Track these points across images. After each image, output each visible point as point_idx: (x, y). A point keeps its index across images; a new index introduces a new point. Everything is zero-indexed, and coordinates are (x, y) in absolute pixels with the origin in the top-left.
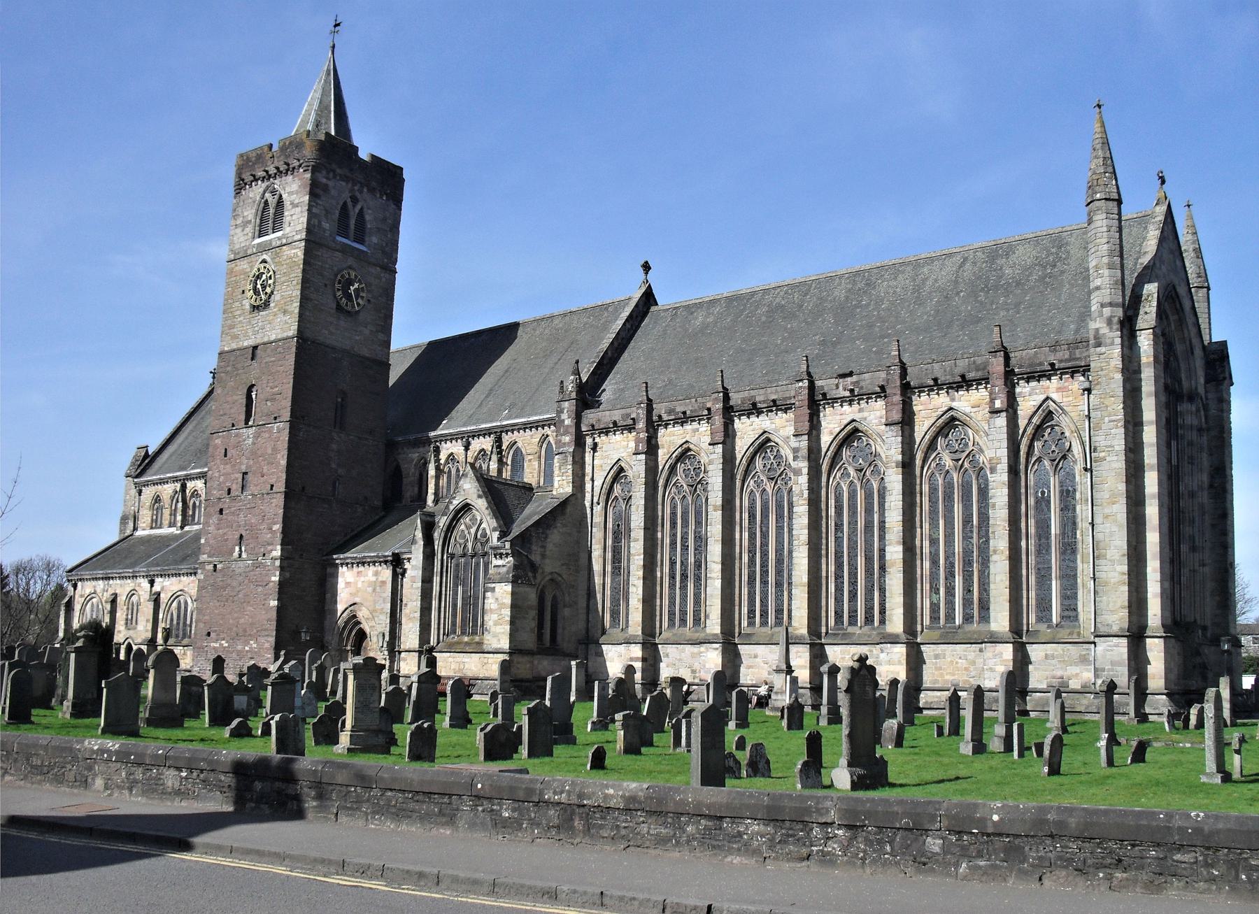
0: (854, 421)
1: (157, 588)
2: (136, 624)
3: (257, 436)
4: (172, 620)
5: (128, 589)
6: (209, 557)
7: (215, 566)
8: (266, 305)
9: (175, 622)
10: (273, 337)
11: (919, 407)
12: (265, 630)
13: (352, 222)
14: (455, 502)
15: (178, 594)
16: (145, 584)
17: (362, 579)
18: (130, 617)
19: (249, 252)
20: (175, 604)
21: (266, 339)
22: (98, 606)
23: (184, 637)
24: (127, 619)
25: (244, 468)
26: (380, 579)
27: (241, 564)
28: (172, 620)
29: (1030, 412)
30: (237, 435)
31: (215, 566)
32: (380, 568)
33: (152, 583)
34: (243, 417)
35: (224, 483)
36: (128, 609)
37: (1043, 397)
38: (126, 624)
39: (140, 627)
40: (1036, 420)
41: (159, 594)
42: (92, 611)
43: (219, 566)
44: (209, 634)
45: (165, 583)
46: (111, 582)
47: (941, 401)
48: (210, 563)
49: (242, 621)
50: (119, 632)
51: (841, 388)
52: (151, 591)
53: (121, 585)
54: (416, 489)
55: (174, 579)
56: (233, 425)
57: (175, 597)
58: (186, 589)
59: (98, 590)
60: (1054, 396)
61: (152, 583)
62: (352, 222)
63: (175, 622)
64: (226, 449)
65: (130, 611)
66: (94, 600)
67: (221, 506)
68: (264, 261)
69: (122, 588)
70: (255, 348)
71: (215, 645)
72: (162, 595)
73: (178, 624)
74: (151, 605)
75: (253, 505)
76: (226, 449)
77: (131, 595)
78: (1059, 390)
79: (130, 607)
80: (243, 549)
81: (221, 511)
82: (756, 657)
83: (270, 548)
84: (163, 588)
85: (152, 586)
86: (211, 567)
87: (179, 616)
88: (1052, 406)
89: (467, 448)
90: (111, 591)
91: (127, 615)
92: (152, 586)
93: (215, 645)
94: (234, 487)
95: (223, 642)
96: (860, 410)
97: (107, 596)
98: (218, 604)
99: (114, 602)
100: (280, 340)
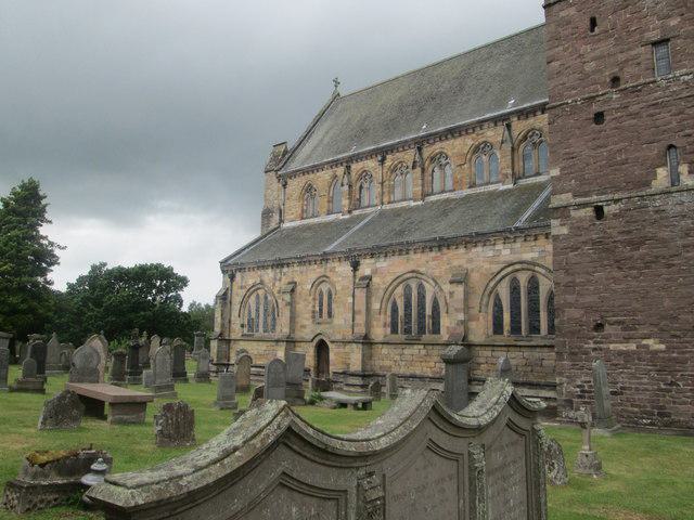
1: (366, 268)
6: (575, 196)
7: (599, 211)
9: (401, 312)
15: (405, 276)
16: (345, 268)
18: (317, 309)
20: (400, 290)
22: (266, 298)
23: (422, 330)
24: (314, 312)
25: (655, 35)
28: (395, 310)
31: (599, 211)
33: (355, 266)
35: (598, 71)
36: (314, 299)
38: (314, 317)
42: (258, 303)
44: (599, 327)
45: (378, 265)
46: (285, 269)
50: (303, 327)
52: (355, 276)
53: (301, 273)
57: (400, 280)
58: (422, 270)
61: (355, 266)
63: (401, 312)
65: (317, 302)
66: (261, 292)
67: (595, 108)
69: (306, 277)
72: (374, 280)
73: (408, 315)
74: (361, 294)
77: (323, 279)
79: (318, 297)
81: (599, 118)
84: (375, 271)
86: (589, 212)
87: (408, 305)
90: (285, 280)
91: (314, 306)
93: (622, 347)
95: (650, 342)
97: (283, 284)
98: (619, 274)
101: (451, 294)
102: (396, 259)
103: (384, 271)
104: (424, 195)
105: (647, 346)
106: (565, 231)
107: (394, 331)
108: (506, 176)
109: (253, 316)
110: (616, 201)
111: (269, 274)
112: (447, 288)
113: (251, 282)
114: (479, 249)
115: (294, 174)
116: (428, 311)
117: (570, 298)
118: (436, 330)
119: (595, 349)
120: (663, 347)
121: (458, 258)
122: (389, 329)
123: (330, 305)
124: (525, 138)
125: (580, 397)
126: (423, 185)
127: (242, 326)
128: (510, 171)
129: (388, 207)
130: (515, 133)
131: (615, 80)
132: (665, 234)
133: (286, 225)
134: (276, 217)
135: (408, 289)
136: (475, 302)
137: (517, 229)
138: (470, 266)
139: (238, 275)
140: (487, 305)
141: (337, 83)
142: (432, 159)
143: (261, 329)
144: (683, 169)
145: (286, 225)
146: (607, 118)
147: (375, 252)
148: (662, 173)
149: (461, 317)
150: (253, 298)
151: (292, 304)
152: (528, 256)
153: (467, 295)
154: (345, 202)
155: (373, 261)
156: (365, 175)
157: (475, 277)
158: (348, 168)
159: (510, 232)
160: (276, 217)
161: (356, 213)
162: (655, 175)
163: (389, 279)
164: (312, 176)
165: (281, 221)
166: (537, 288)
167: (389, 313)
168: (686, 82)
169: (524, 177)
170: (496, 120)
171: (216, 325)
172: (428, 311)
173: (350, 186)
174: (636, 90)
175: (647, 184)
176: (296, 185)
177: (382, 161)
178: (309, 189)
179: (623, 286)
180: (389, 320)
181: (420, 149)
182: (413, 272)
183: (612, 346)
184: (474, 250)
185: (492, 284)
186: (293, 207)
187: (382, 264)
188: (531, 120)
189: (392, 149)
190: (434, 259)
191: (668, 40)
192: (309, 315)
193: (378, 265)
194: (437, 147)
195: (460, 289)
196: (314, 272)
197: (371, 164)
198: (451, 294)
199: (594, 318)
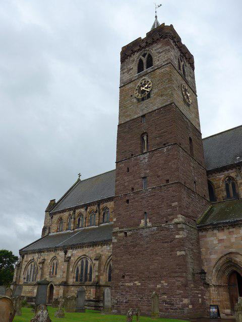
1: (69, 254)
2: (56, 274)
3: (150, 158)
4: (78, 271)
5: (52, 256)
7: (126, 233)
8: (149, 96)
9: (80, 272)
10: (156, 108)
12: (175, 272)
13: (182, 68)
16: (62, 253)
17: (235, 236)
18: (52, 271)
20: (80, 263)
21: (150, 111)
22: (34, 266)
23: (86, 280)
25: (143, 175)
28: (78, 271)
30: (136, 160)
31: (126, 233)
33: (66, 253)
34: (139, 149)
35: (128, 186)
38: (50, 274)
39: (58, 276)
41: (70, 258)
42: (31, 268)
43: (129, 233)
44: (123, 277)
45: (73, 252)
46: (42, 254)
48: (121, 232)
49: (152, 267)
52: (65, 257)
53: (48, 255)
54: (225, 194)
55: (79, 250)
56: (132, 155)
57: (80, 258)
59: (35, 258)
61: (66, 253)
62: (182, 68)
63: (80, 272)
64: (128, 168)
65: (52, 268)
66: (33, 263)
67: (127, 198)
69: (48, 256)
70: (143, 116)
71: (129, 284)
72: (72, 258)
73: (82, 273)
74: (66, 264)
75: (154, 194)
76: (128, 168)
77: (55, 258)
79: (52, 266)
80: (148, 220)
81: (128, 201)
83: (170, 217)
84: (72, 255)
85: (66, 254)
86: (122, 234)
87: (82, 270)
90: (42, 258)
91: (50, 270)
92: (66, 254)
93: (129, 284)
94: (137, 186)
95: (137, 282)
98: (130, 257)
99: (43, 263)
100: (161, 108)
101: (95, 264)
102: (79, 250)
103: (75, 254)
104: (99, 224)
105: (136, 284)
106: (116, 241)
107: (77, 280)
109: (29, 274)
110: (130, 231)
111: (36, 256)
112: (94, 262)
113: (29, 259)
114: (105, 246)
115: (55, 213)
116: (88, 272)
117: (116, 266)
118: (90, 280)
119: (122, 285)
120: (140, 284)
121: (98, 250)
122: (75, 279)
123: (56, 269)
125: (117, 304)
126: (99, 220)
127: (24, 279)
129: (87, 228)
131: (133, 189)
132: (142, 243)
133: (51, 234)
134: (47, 231)
135: (82, 262)
136: (102, 268)
138: (102, 253)
139: (25, 256)
140: (107, 269)
141: (80, 175)
142: (103, 209)
143: (31, 280)
144: (148, 220)
145: (50, 234)
146: (130, 202)
147: (73, 247)
148: (143, 221)
149: (97, 274)
150: (30, 266)
151: (42, 269)
153: (100, 265)
154: (72, 225)
155: (72, 250)
156: (81, 214)
157: (103, 257)
158: (74, 211)
160: (47, 231)
161: (76, 230)
162: (140, 222)
163: (76, 258)
164: (62, 214)
165: (49, 233)
167: (75, 273)
168: (149, 191)
171: (14, 278)
172: (88, 272)
173: (74, 219)
174: (137, 193)
175: (139, 225)
176: (56, 217)
177: (86, 209)
178: (61, 219)
179: (130, 261)
180: (75, 275)
181: (99, 205)
182: (84, 255)
183: (126, 284)
184: (104, 247)
185: (108, 261)
186: (54, 227)
187: (75, 252)
189: (89, 205)
190: (91, 250)
191: (146, 177)
192: (48, 274)
193: (73, 252)
194: (105, 205)
195: (97, 262)
196: (52, 255)
197: (83, 210)
198: (95, 264)
199: (122, 274)
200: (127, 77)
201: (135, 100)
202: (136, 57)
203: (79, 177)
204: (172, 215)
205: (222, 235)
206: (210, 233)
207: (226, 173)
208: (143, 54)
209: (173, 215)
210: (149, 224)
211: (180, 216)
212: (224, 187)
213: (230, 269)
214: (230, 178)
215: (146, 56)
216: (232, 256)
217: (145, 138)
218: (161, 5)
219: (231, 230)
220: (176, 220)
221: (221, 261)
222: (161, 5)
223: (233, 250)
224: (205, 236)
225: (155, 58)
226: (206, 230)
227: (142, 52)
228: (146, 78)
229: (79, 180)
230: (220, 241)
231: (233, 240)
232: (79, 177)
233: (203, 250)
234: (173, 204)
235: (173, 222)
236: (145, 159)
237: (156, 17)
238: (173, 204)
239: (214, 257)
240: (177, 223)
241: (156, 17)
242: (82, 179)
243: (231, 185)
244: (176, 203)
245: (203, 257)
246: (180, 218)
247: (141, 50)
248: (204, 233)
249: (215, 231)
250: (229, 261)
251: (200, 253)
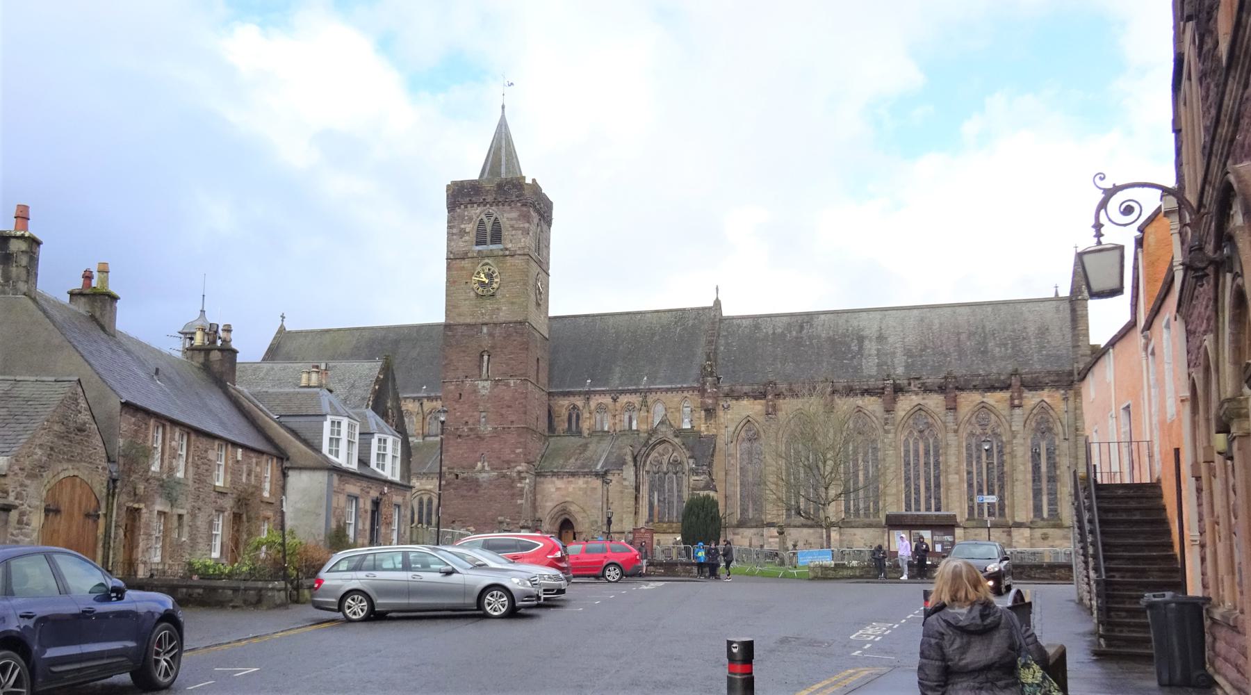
0: (920, 404)
11: (962, 400)
14: (653, 439)
17: (573, 486)
19: (469, 255)
26: (590, 486)
27: (484, 475)
29: (1032, 406)
31: (457, 476)
32: (590, 479)
37: (1039, 400)
40: (1035, 411)
47: (976, 397)
51: (912, 385)
60: (1046, 399)
64: (460, 394)
68: (487, 264)
78: (1049, 396)
82: (855, 535)
83: (513, 465)
88: (1045, 405)
89: (615, 400)
96: (924, 399)
108: (418, 434)
124: (431, 412)
128: (421, 432)
130: (425, 409)
137: (424, 473)
141: (283, 317)
144: (486, 464)
148: (479, 464)
152: (428, 487)
159: (420, 474)
166: (432, 503)
169: (429, 436)
170: (414, 399)
188: (435, 403)
200: (461, 245)
201: (472, 294)
202: (476, 212)
203: (283, 321)
204: (515, 462)
205: (559, 483)
206: (549, 479)
207: (572, 398)
208: (486, 212)
209: (517, 463)
210: (487, 468)
211: (523, 464)
212: (565, 417)
213: (563, 517)
214: (575, 407)
215: (493, 219)
216: (566, 504)
217: (486, 358)
218: (512, 84)
219: (570, 479)
220: (519, 468)
221: (556, 510)
222: (512, 84)
223: (568, 499)
224: (543, 483)
225: (505, 233)
226: (545, 476)
227: (489, 209)
228: (490, 262)
229: (282, 330)
230: (558, 489)
231: (571, 489)
232: (283, 321)
233: (539, 497)
234: (518, 451)
235: (516, 470)
236: (484, 387)
237: (503, 107)
238: (518, 451)
239: (550, 505)
240: (519, 472)
241: (503, 107)
242: (290, 327)
243: (574, 416)
244: (521, 450)
245: (537, 504)
246: (522, 467)
247: (485, 205)
248: (542, 479)
249: (554, 479)
250: (564, 510)
251: (535, 499)
